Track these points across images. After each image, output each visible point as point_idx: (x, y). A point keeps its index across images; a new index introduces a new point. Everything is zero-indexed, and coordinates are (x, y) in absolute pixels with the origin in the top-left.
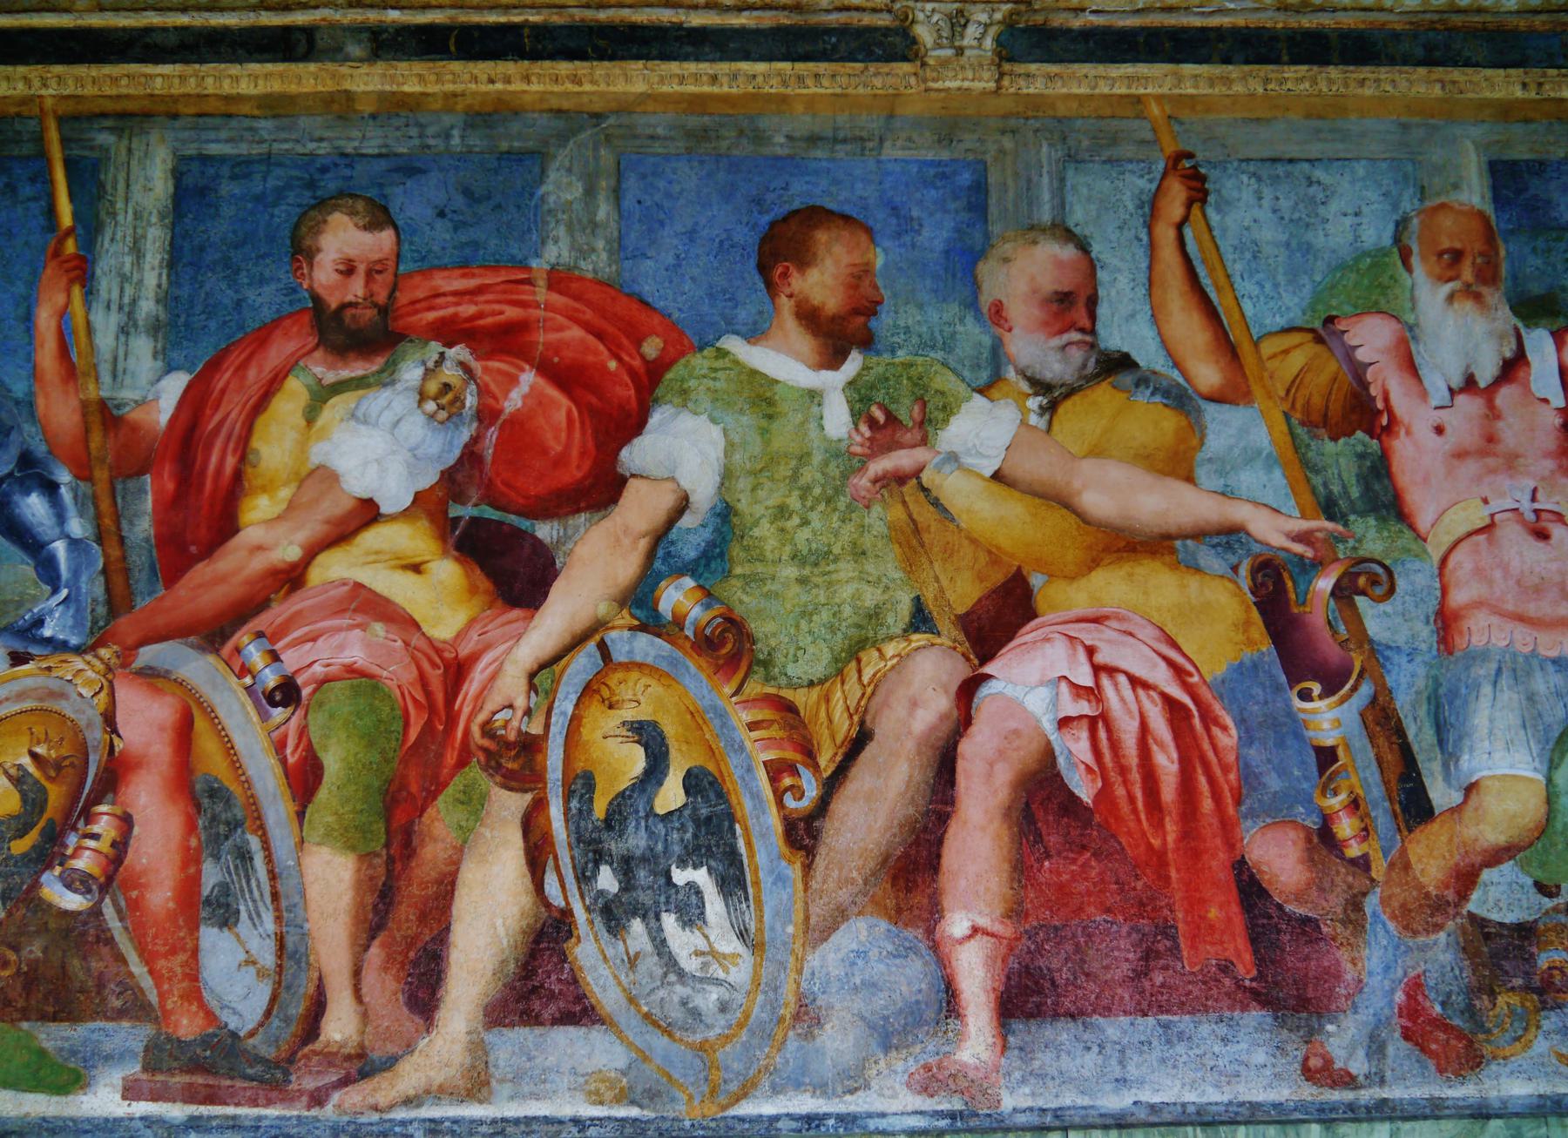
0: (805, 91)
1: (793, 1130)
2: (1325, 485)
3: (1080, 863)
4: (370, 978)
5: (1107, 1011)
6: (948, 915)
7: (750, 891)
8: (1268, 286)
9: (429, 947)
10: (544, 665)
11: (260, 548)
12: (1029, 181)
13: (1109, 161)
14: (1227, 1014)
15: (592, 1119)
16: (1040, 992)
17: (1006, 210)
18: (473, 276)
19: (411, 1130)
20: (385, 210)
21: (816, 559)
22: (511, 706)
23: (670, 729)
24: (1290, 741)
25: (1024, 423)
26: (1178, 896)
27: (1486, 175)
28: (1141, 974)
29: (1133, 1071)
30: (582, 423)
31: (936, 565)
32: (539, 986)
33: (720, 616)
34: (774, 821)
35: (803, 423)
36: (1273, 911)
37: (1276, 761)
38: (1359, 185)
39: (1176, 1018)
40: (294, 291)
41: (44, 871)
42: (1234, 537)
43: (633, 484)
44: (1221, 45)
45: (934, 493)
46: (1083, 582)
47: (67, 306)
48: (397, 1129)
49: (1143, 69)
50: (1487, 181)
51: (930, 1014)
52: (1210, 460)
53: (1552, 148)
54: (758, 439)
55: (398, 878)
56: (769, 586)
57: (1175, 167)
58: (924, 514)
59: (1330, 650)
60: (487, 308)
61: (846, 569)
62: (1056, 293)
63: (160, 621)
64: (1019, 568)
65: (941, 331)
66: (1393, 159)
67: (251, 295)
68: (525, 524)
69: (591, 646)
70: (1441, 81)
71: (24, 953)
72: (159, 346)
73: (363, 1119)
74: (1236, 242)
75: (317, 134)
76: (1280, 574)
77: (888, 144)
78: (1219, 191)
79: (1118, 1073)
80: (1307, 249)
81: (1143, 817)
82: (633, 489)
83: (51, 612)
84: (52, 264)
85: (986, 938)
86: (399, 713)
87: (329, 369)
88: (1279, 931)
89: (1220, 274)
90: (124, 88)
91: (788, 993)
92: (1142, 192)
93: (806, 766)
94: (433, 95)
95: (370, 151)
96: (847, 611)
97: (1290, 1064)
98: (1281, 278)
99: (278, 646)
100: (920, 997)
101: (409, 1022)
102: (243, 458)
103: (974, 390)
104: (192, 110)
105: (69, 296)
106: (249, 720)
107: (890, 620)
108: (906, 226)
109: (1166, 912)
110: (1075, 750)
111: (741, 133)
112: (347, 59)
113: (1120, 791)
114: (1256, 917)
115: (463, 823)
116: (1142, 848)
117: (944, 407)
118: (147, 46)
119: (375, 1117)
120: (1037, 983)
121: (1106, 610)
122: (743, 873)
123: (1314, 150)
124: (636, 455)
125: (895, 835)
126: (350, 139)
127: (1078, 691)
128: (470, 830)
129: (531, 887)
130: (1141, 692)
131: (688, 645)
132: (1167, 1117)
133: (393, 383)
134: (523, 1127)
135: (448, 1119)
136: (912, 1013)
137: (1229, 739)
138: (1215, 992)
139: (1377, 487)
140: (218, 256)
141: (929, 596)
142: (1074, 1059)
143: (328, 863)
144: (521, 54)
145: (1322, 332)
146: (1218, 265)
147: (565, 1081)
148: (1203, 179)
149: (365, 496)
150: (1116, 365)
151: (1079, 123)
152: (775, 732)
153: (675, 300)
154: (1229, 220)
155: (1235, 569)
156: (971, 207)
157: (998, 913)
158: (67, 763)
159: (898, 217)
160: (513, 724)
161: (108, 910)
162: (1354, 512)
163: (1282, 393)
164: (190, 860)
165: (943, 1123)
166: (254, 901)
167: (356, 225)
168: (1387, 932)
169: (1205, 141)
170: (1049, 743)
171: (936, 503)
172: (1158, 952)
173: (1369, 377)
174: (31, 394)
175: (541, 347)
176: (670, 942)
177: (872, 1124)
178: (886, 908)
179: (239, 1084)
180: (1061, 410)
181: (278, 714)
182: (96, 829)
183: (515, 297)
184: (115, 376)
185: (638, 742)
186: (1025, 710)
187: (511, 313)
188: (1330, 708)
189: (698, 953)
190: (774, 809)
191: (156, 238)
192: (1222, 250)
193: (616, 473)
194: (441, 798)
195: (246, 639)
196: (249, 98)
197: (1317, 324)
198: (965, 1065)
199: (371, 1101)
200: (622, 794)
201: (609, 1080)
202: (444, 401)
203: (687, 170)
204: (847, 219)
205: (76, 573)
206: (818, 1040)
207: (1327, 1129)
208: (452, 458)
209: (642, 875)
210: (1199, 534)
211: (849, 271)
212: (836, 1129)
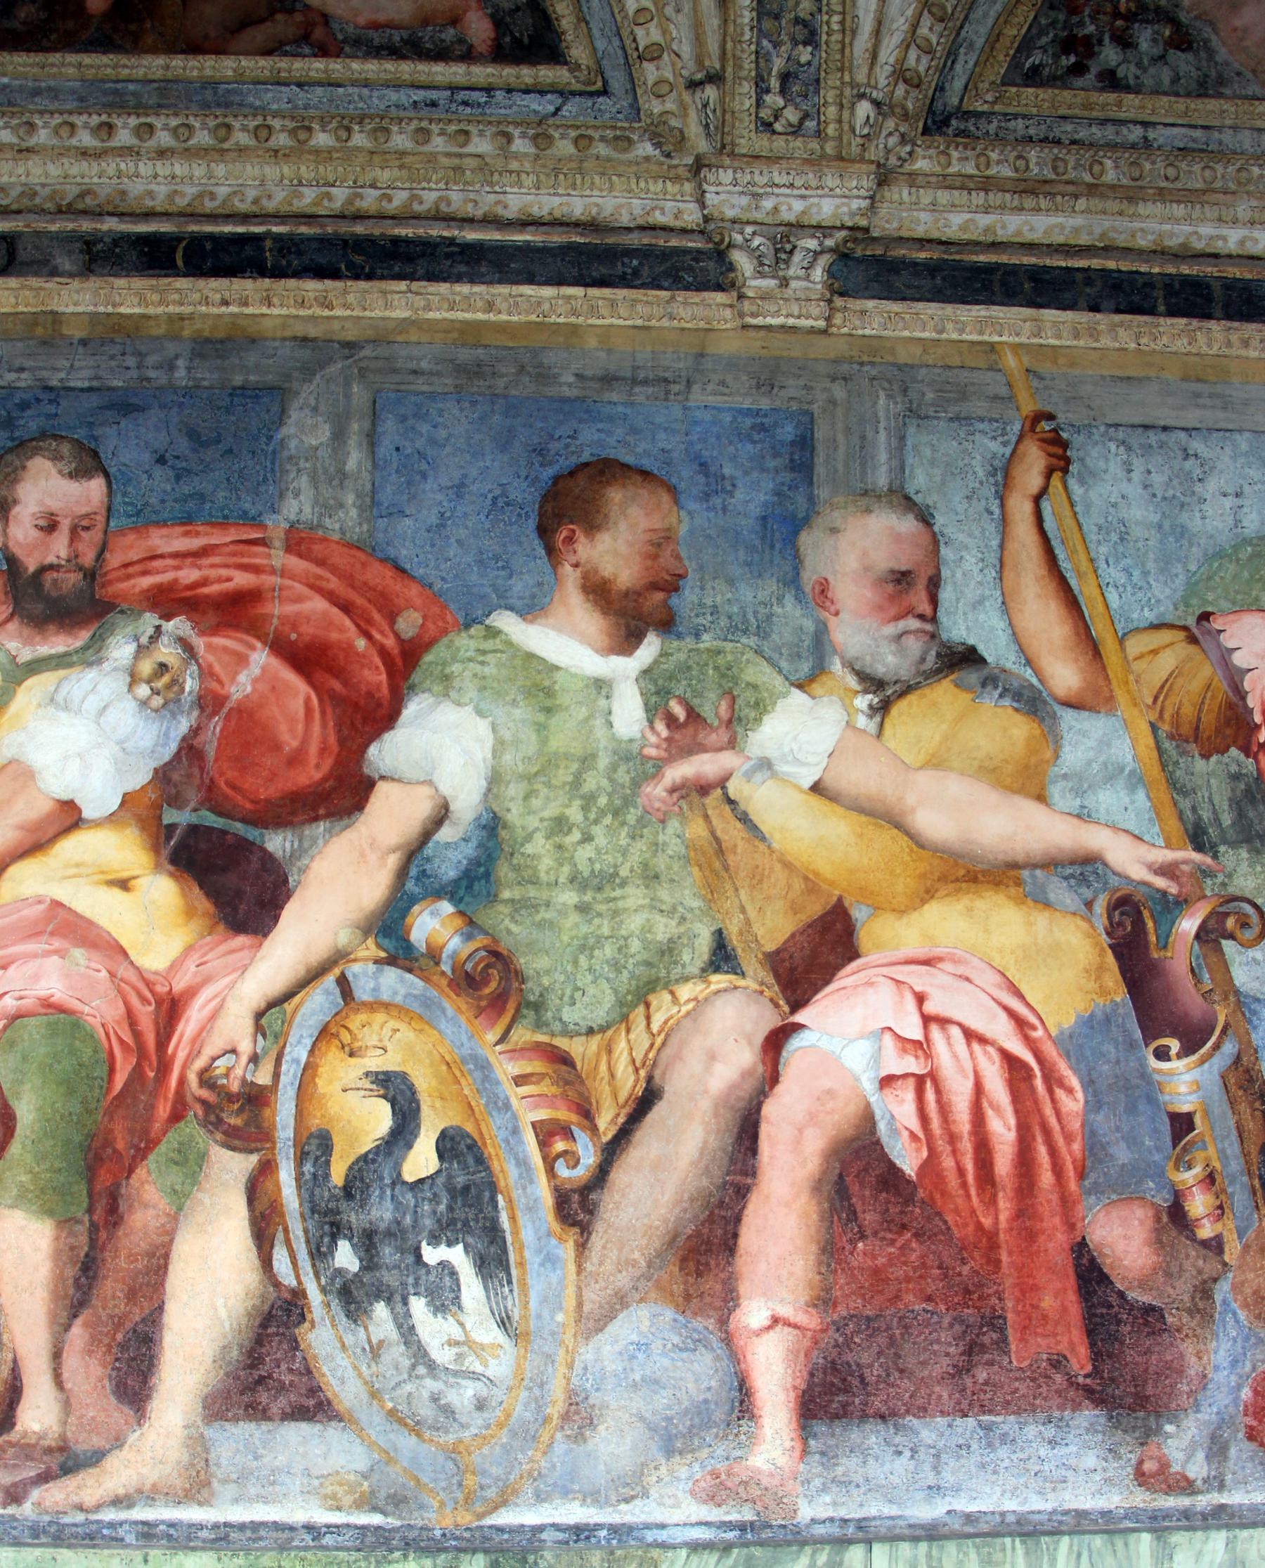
0: (599, 322)
1: (559, 1542)
2: (1194, 809)
3: (898, 1244)
4: (72, 1362)
5: (922, 1411)
6: (744, 1303)
7: (514, 1272)
8: (1136, 573)
9: (140, 1328)
10: (271, 1005)
12: (863, 438)
13: (957, 418)
14: (1057, 1414)
15: (328, 1526)
16: (846, 1391)
17: (836, 471)
18: (197, 534)
19: (121, 1532)
20: (95, 454)
21: (601, 882)
22: (233, 1051)
23: (423, 1081)
24: (1142, 1106)
25: (849, 725)
26: (1009, 1282)
28: (961, 1371)
29: (948, 1477)
30: (323, 713)
31: (742, 892)
32: (268, 1375)
33: (484, 948)
34: (543, 1192)
35: (587, 719)
36: (1114, 1300)
37: (1125, 1129)
38: (1241, 460)
39: (999, 1419)
42: (1089, 868)
43: (381, 787)
44: (1088, 290)
45: (742, 807)
46: (915, 916)
48: (105, 1532)
49: (997, 311)
51: (719, 1415)
52: (1065, 776)
54: (534, 737)
55: (103, 1249)
56: (543, 914)
57: (1033, 430)
58: (731, 832)
59: (1190, 999)
60: (213, 573)
61: (634, 896)
62: (892, 572)
64: (840, 899)
65: (755, 613)
68: (252, 833)
69: (330, 980)
73: (67, 1520)
74: (1102, 521)
75: (17, 363)
76: (1140, 913)
77: (696, 388)
78: (1082, 460)
79: (931, 1479)
80: (1182, 532)
81: (973, 1192)
82: (383, 799)
85: (787, 1330)
86: (104, 1056)
88: (1119, 1322)
89: (1082, 557)
91: (557, 1391)
92: (994, 456)
93: (583, 1128)
94: (157, 317)
95: (79, 384)
96: (635, 945)
97: (1123, 1468)
98: (1151, 565)
100: (709, 1396)
101: (119, 1414)
103: (792, 684)
107: (686, 957)
108: (715, 486)
109: (994, 1300)
110: (898, 1111)
111: (522, 369)
112: (54, 273)
113: (948, 1163)
114: (1093, 1305)
115: (178, 1187)
116: (971, 1228)
117: (757, 704)
119: (80, 1518)
120: (844, 1380)
121: (938, 951)
122: (505, 1251)
123: (1192, 417)
124: (385, 753)
125: (685, 1211)
126: (54, 369)
127: (906, 1045)
128: (187, 1196)
129: (257, 1262)
130: (976, 1047)
131: (444, 982)
132: (984, 1528)
133: (99, 662)
134: (249, 1533)
135: (163, 1522)
136: (699, 1413)
137: (1073, 1104)
138: (1044, 1389)
139: (1251, 814)
141: (733, 930)
142: (882, 1465)
143: (22, 1229)
144: (261, 270)
145: (1195, 631)
146: (1080, 547)
147: (296, 1484)
148: (1065, 445)
149: (65, 797)
150: (960, 659)
151: (923, 371)
152: (546, 1088)
153: (437, 568)
154: (1093, 495)
155: (1089, 905)
156: (793, 467)
157: (802, 1300)
159: (707, 475)
160: (235, 1072)
162: (1225, 842)
163: (1149, 701)
165: (731, 1535)
167: (60, 472)
168: (1237, 1321)
169: (1067, 401)
170: (868, 1105)
171: (744, 819)
172: (983, 1345)
173: (1247, 685)
175: (275, 621)
176: (420, 1329)
177: (650, 1536)
178: (672, 1295)
180: (895, 711)
183: (246, 560)
185: (384, 1097)
186: (842, 1066)
187: (242, 580)
188: (1189, 1070)
189: (452, 1343)
190: (542, 1179)
192: (1085, 527)
193: (362, 775)
194: (152, 1157)
197: (1191, 621)
198: (759, 1471)
199: (75, 1499)
200: (364, 1158)
201: (348, 1483)
202: (159, 684)
203: (456, 411)
204: (645, 474)
206: (590, 1444)
207: (1158, 1538)
208: (167, 753)
209: (388, 1253)
210: (1051, 863)
211: (647, 537)
212: (608, 1541)
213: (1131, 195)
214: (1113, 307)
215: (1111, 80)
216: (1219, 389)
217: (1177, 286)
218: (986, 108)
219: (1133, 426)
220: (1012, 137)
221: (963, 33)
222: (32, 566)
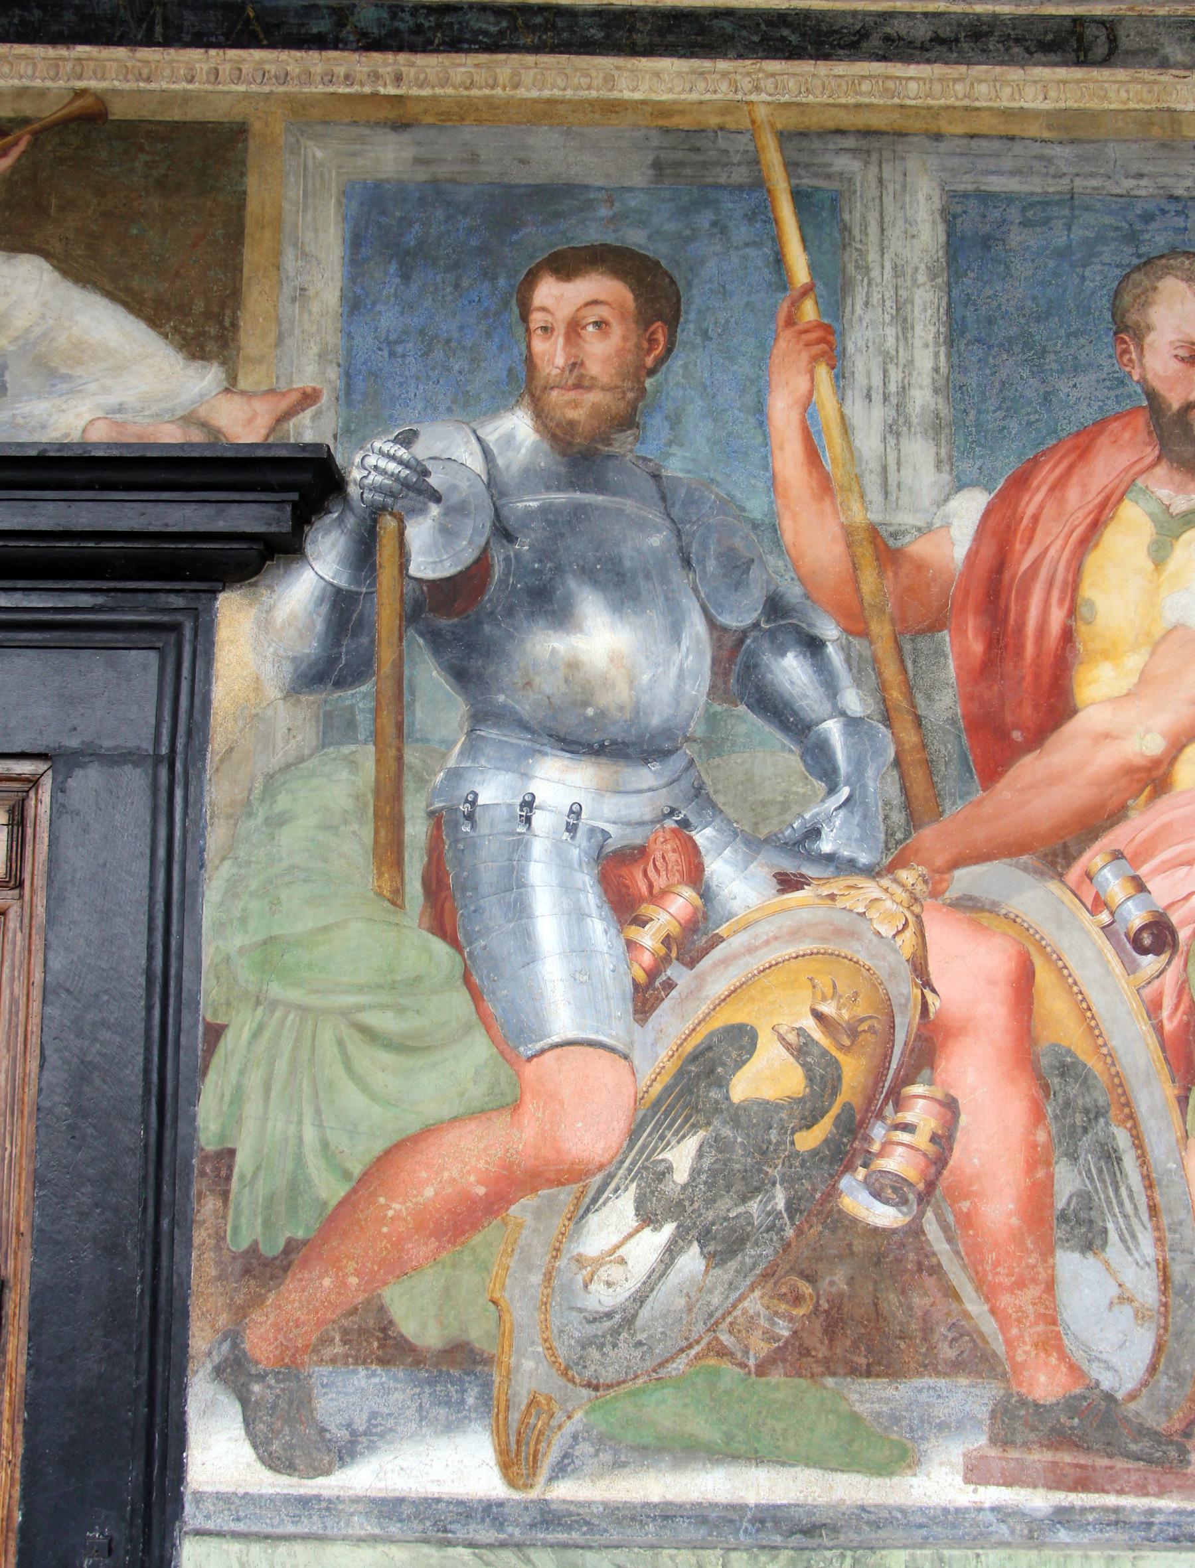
11: (1107, 736)
40: (1121, 383)
41: (843, 1173)
47: (811, 392)
63: (979, 834)
67: (1063, 386)
71: (824, 1285)
72: (943, 452)
75: (1134, 167)
83: (829, 818)
84: (786, 335)
87: (1177, 492)
90: (867, 94)
99: (1142, 871)
102: (1072, 612)
104: (960, 129)
105: (812, 380)
106: (1109, 972)
112: (1165, 64)
118: (887, 39)
140: (1013, 331)
158: (864, 1026)
161: (932, 1229)
164: (1037, 1159)
166: (1126, 1217)
174: (773, 514)
179: (1121, 1464)
181: (1149, 963)
182: (908, 1117)
184: (886, 494)
191: (926, 303)
195: (1099, 861)
196: (1036, 114)
205: (859, 765)
222: (1175, 402)
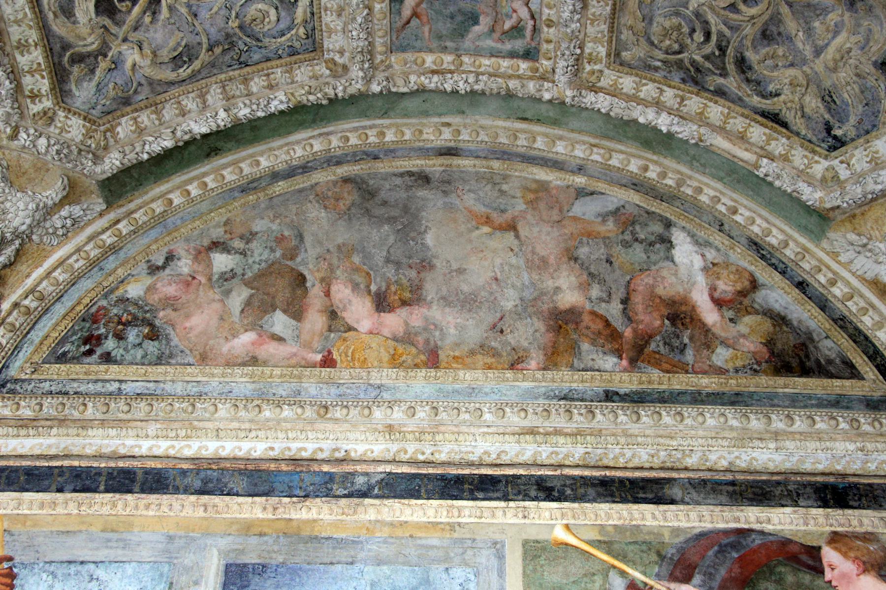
27: (221, 574)
38: (126, 580)
44: (59, 479)
50: (221, 579)
53: (274, 555)
66: (155, 562)
70: (205, 506)
123: (100, 555)
169: (24, 548)
213: (84, 425)
214: (72, 488)
215: (107, 358)
216: (124, 536)
217: (115, 474)
218: (27, 377)
219: (62, 562)
220: (40, 392)
221: (29, 336)
